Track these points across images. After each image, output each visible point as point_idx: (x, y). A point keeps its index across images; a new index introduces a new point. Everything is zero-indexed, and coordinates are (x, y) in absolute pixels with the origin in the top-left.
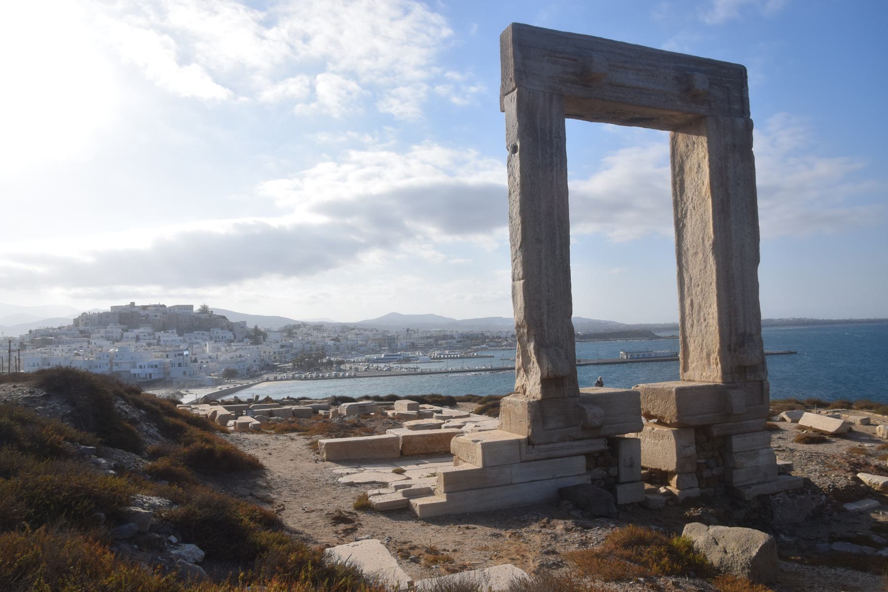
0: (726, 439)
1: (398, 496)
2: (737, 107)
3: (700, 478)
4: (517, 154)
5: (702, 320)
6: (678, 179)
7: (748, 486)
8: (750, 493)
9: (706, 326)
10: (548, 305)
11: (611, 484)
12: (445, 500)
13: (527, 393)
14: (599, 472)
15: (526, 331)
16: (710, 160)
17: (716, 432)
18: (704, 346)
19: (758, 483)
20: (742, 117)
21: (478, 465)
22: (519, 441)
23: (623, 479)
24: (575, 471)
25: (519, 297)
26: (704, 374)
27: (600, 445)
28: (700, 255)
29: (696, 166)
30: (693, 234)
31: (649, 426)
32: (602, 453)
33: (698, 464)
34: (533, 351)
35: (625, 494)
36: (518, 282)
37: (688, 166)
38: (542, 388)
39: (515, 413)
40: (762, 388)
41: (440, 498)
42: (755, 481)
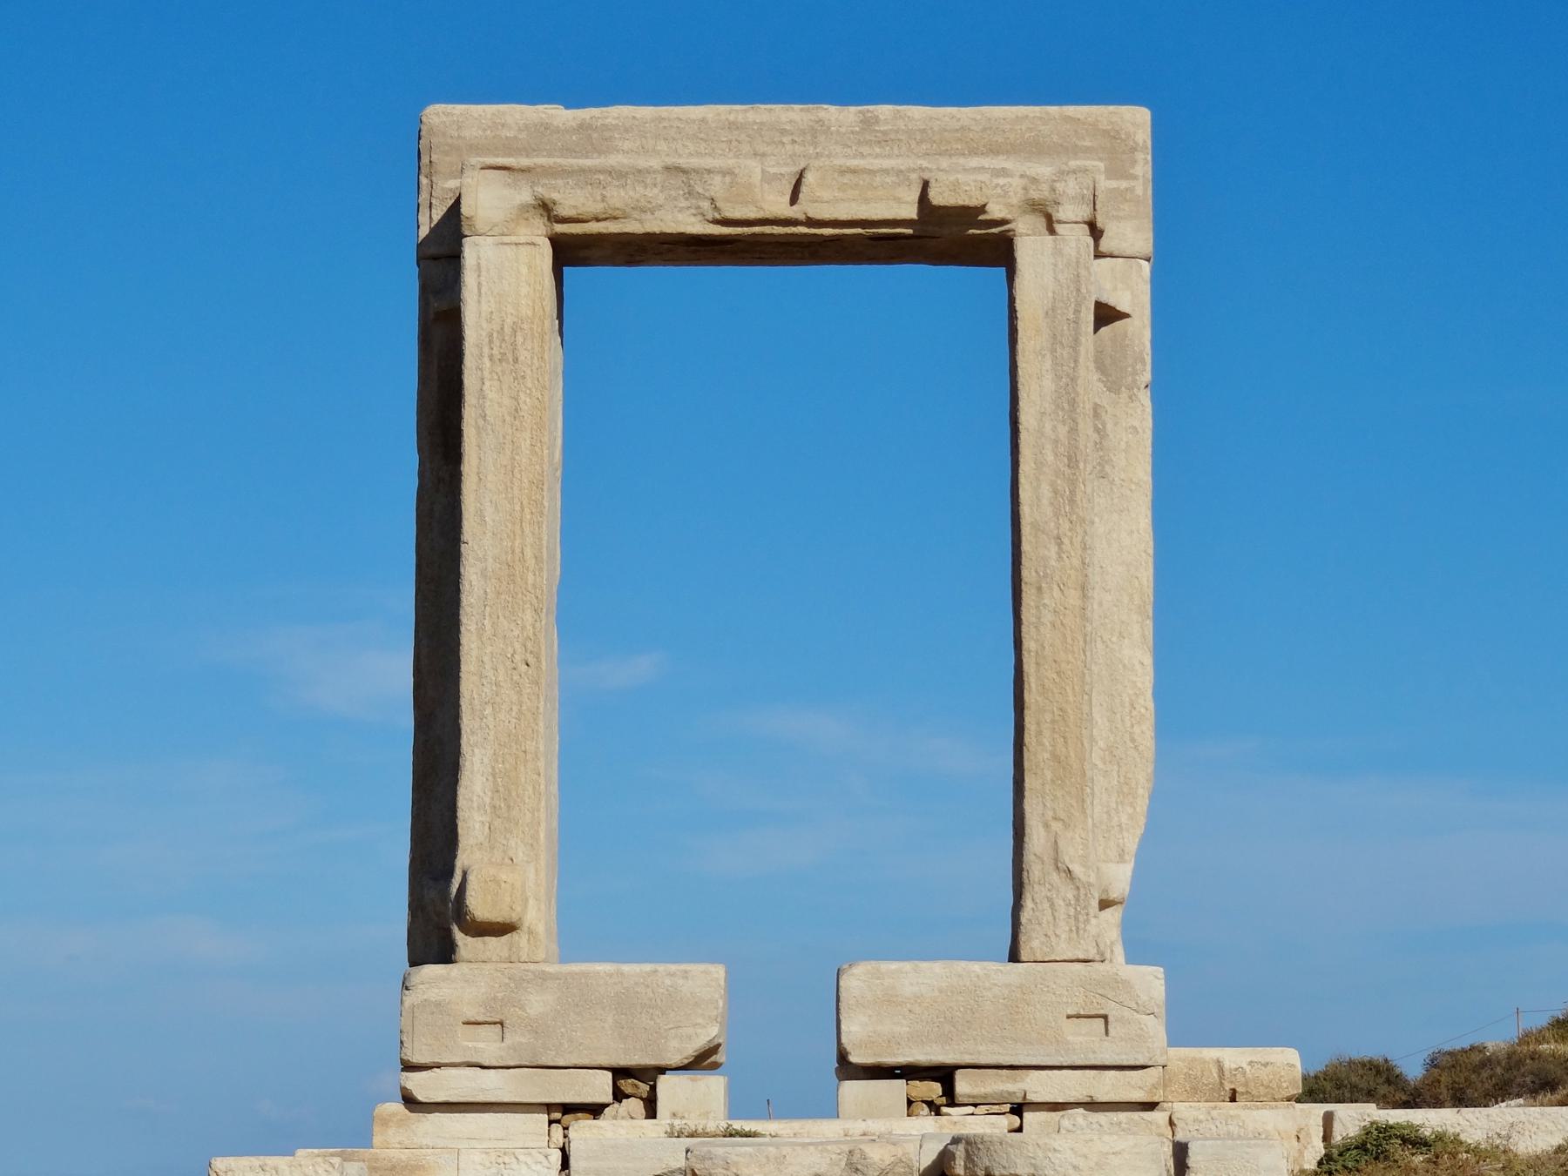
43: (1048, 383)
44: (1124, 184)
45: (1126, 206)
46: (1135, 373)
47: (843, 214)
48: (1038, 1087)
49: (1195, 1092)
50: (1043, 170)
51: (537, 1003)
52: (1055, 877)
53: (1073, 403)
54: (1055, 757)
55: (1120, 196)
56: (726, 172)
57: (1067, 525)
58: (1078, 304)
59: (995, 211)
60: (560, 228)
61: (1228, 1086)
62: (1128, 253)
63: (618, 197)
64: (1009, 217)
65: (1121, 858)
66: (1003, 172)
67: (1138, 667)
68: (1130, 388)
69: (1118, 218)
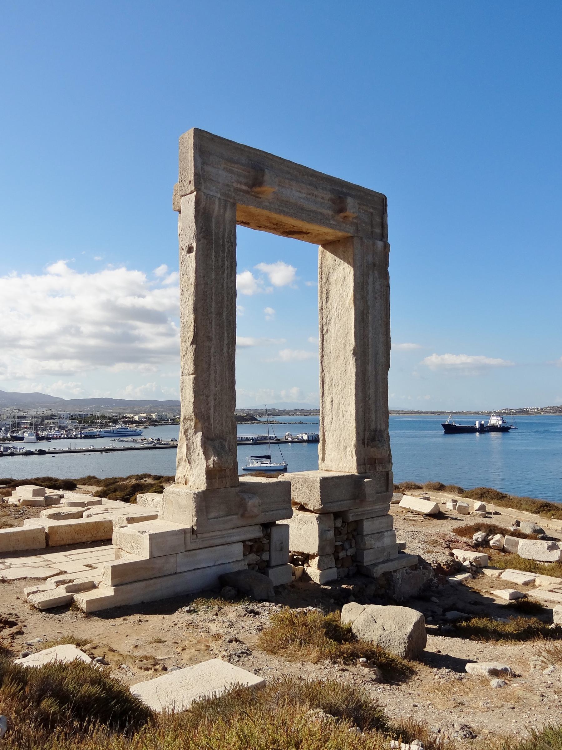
0: (358, 524)
1: (61, 592)
2: (378, 230)
3: (337, 559)
4: (193, 255)
5: (341, 415)
6: (324, 289)
7: (375, 565)
8: (379, 571)
9: (344, 422)
10: (215, 399)
11: (264, 567)
12: (112, 593)
13: (190, 483)
14: (253, 557)
15: (193, 424)
16: (355, 275)
17: (351, 518)
18: (342, 440)
19: (383, 562)
20: (381, 240)
21: (145, 555)
22: (184, 531)
23: (273, 563)
24: (232, 556)
25: (188, 391)
26: (341, 465)
27: (256, 533)
28: (342, 358)
29: (342, 280)
31: (297, 513)
32: (255, 540)
33: (336, 546)
34: (199, 444)
35: (276, 576)
36: (188, 377)
37: (335, 279)
38: (207, 479)
39: (178, 503)
40: (388, 476)
41: (106, 590)
42: (380, 560)
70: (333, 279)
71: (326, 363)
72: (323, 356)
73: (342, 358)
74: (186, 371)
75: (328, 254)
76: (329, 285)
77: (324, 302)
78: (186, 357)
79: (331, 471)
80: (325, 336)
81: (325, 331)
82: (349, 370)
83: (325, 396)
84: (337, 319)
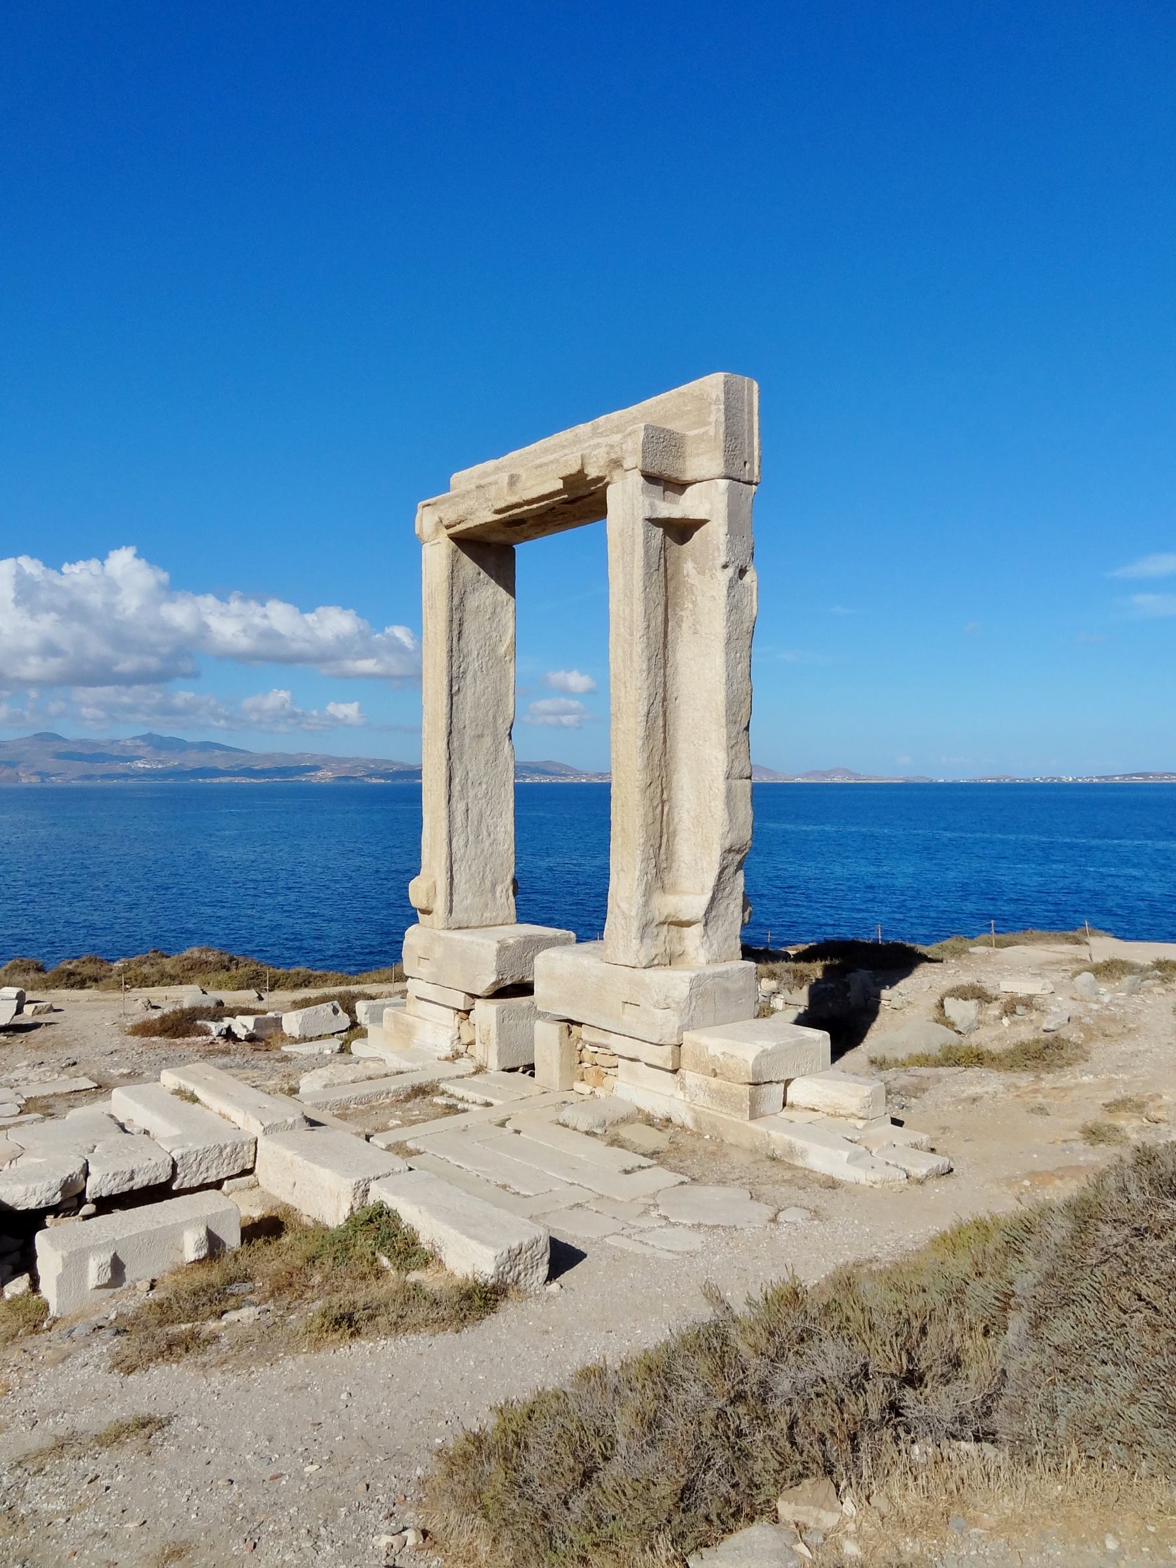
6: (456, 617)
9: (491, 844)
28: (488, 741)
30: (477, 706)
36: (739, 782)
39: (727, 991)
43: (621, 581)
44: (702, 431)
45: (703, 446)
46: (714, 559)
47: (534, 494)
48: (619, 1045)
49: (698, 1066)
50: (616, 438)
51: (438, 952)
52: (616, 910)
53: (631, 592)
54: (623, 829)
55: (701, 438)
56: (496, 483)
57: (628, 674)
58: (634, 523)
59: (592, 472)
60: (452, 531)
61: (711, 1067)
62: (708, 477)
63: (461, 509)
64: (601, 474)
65: (703, 892)
66: (598, 445)
67: (714, 760)
68: (711, 570)
69: (698, 455)
70: (472, 603)
71: (456, 744)
72: (450, 733)
73: (488, 741)
74: (736, 771)
75: (465, 558)
76: (463, 611)
77: (455, 639)
78: (737, 748)
79: (467, 928)
80: (455, 698)
81: (455, 688)
82: (501, 760)
83: (453, 800)
84: (479, 673)
